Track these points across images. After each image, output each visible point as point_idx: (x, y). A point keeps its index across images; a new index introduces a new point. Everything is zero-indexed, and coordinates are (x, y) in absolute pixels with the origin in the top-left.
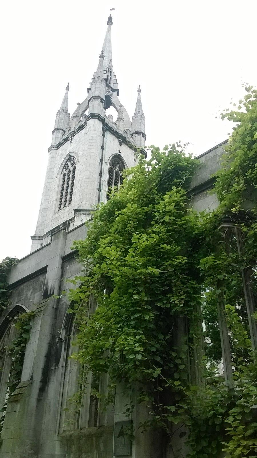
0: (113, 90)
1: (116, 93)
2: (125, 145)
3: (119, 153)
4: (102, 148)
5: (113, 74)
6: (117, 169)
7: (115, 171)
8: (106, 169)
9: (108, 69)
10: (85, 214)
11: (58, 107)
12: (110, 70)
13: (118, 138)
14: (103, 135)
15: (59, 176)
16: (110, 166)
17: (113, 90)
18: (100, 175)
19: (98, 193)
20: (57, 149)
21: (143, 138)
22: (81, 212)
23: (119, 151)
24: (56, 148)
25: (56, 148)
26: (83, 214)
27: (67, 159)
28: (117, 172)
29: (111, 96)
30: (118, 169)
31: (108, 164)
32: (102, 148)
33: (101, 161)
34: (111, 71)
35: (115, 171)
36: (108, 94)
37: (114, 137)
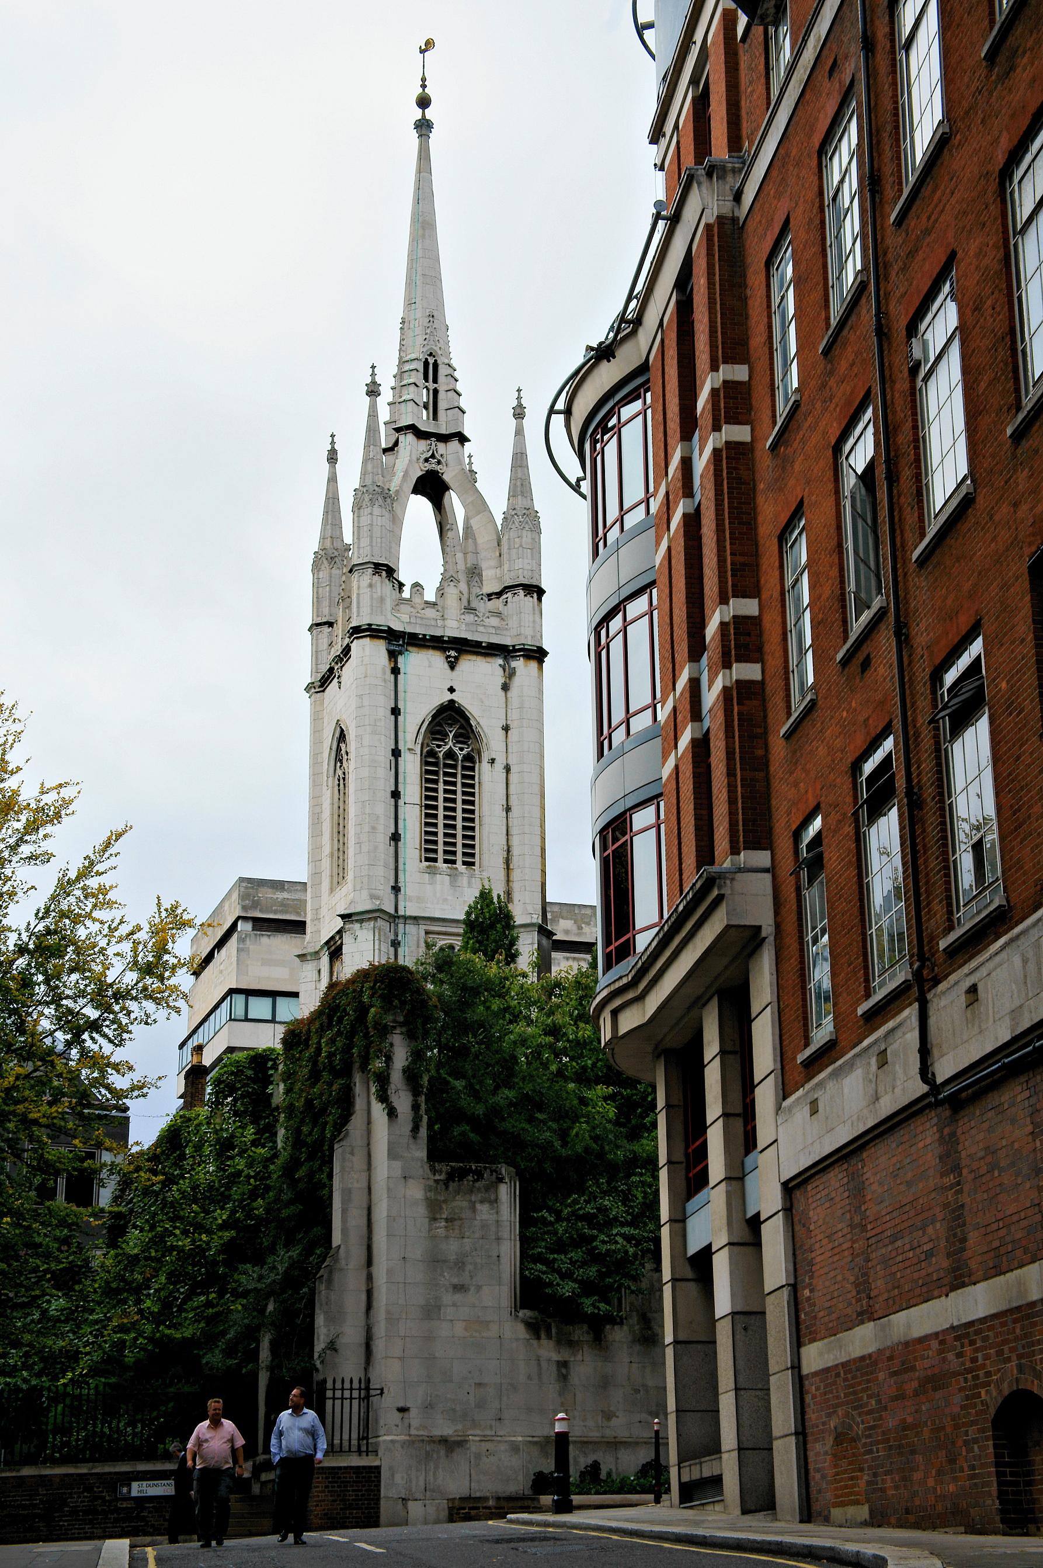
0: (444, 438)
1: (454, 444)
2: (474, 658)
3: (449, 696)
4: (395, 711)
5: (443, 371)
6: (447, 747)
7: (441, 755)
8: (411, 765)
9: (426, 364)
10: (361, 921)
11: (312, 543)
12: (431, 361)
13: (444, 650)
14: (396, 671)
15: (331, 779)
16: (425, 750)
17: (444, 438)
18: (396, 795)
19: (392, 849)
20: (323, 691)
21: (530, 601)
22: (354, 918)
23: (452, 690)
24: (320, 687)
25: (320, 687)
26: (357, 921)
27: (337, 735)
28: (450, 755)
29: (438, 468)
30: (451, 744)
31: (418, 751)
32: (395, 711)
33: (396, 753)
34: (436, 365)
35: (441, 755)
36: (428, 466)
37: (431, 652)
